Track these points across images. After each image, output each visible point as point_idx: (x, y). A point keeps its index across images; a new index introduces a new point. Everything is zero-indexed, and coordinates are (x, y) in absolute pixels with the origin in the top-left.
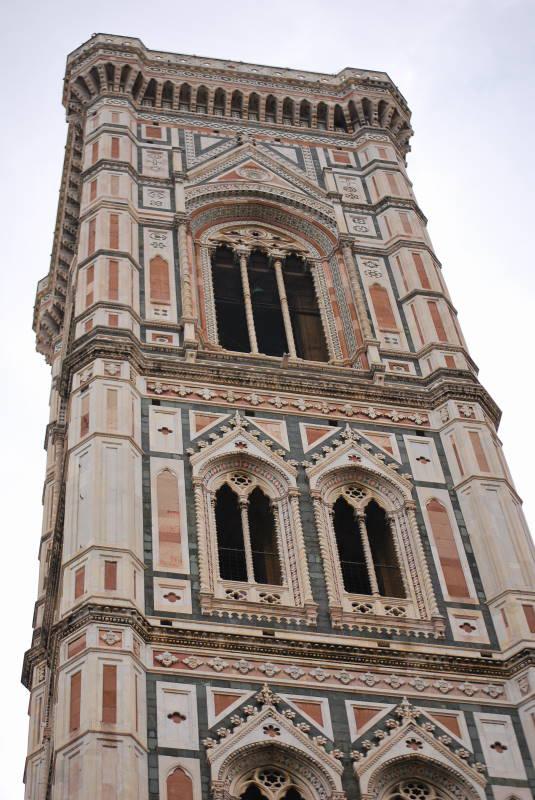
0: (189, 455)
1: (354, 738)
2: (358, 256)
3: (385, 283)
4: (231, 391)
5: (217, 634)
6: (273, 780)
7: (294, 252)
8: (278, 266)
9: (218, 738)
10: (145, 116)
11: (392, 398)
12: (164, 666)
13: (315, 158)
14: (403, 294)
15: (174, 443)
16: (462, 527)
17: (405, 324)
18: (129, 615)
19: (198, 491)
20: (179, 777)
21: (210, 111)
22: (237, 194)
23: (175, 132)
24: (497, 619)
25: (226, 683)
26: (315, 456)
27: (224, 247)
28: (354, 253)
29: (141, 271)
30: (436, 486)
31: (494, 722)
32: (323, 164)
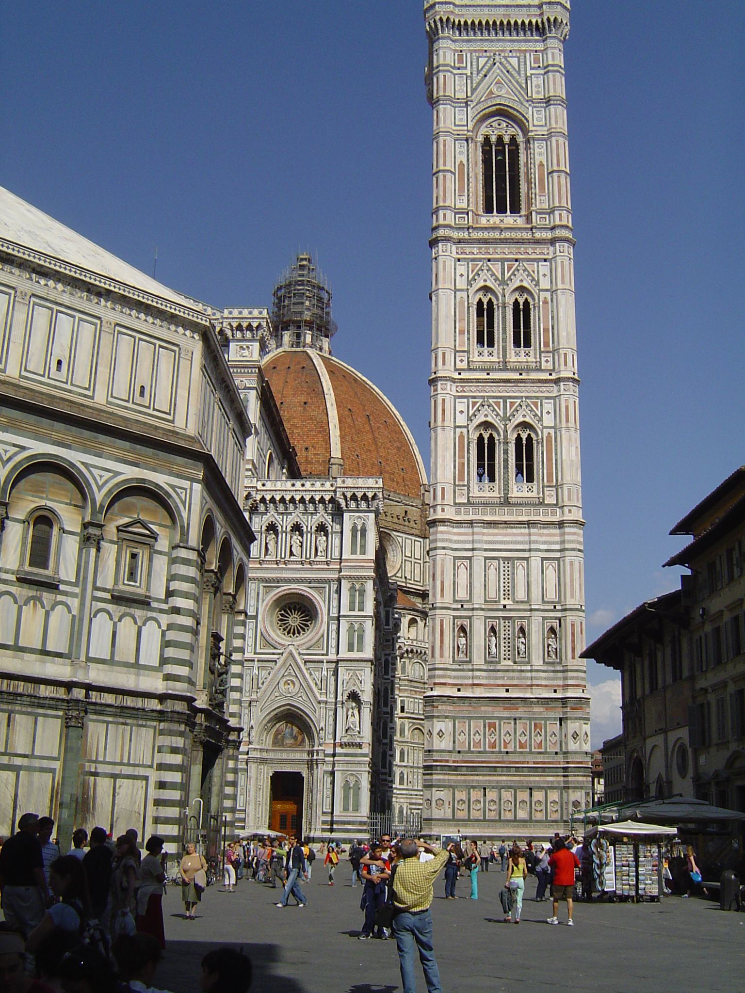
1: (508, 415)
3: (545, 163)
7: (513, 136)
8: (507, 146)
11: (538, 242)
13: (525, 64)
14: (549, 171)
16: (552, 311)
17: (548, 189)
20: (461, 437)
23: (469, 55)
24: (556, 357)
25: (474, 397)
26: (509, 282)
29: (455, 174)
30: (547, 290)
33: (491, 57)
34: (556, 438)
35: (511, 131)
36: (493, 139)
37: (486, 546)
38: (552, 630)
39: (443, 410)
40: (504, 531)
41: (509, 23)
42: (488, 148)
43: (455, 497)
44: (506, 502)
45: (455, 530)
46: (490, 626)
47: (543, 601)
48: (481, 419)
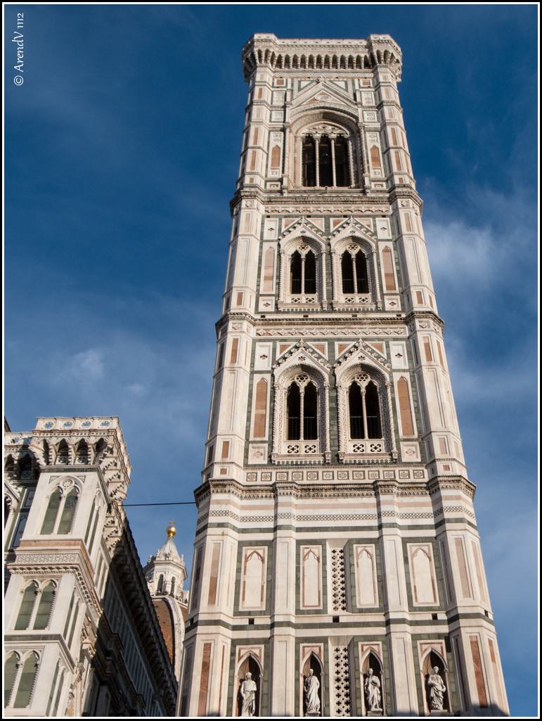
0: (280, 240)
1: (336, 358)
2: (367, 133)
4: (301, 207)
5: (283, 319)
6: (302, 379)
7: (340, 134)
9: (279, 364)
10: (277, 74)
11: (372, 201)
12: (260, 335)
13: (353, 84)
15: (273, 235)
17: (384, 164)
18: (244, 315)
19: (282, 255)
20: (262, 384)
21: (307, 67)
22: (315, 108)
25: (285, 340)
26: (335, 233)
27: (309, 136)
28: (365, 133)
29: (268, 154)
31: (398, 345)
32: (357, 87)
33: (312, 81)
34: (413, 383)
35: (339, 131)
36: (318, 136)
37: (296, 524)
38: (434, 659)
39: (235, 352)
40: (333, 501)
41: (335, 58)
42: (310, 145)
43: (246, 457)
44: (337, 460)
45: (246, 502)
46: (308, 656)
47: (412, 609)
48: (294, 360)
